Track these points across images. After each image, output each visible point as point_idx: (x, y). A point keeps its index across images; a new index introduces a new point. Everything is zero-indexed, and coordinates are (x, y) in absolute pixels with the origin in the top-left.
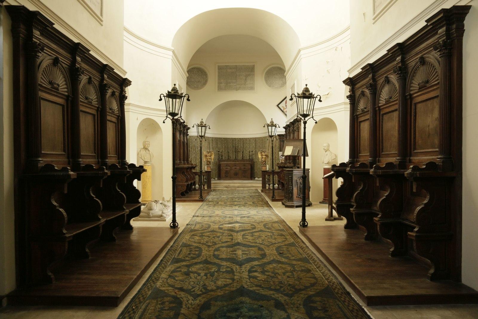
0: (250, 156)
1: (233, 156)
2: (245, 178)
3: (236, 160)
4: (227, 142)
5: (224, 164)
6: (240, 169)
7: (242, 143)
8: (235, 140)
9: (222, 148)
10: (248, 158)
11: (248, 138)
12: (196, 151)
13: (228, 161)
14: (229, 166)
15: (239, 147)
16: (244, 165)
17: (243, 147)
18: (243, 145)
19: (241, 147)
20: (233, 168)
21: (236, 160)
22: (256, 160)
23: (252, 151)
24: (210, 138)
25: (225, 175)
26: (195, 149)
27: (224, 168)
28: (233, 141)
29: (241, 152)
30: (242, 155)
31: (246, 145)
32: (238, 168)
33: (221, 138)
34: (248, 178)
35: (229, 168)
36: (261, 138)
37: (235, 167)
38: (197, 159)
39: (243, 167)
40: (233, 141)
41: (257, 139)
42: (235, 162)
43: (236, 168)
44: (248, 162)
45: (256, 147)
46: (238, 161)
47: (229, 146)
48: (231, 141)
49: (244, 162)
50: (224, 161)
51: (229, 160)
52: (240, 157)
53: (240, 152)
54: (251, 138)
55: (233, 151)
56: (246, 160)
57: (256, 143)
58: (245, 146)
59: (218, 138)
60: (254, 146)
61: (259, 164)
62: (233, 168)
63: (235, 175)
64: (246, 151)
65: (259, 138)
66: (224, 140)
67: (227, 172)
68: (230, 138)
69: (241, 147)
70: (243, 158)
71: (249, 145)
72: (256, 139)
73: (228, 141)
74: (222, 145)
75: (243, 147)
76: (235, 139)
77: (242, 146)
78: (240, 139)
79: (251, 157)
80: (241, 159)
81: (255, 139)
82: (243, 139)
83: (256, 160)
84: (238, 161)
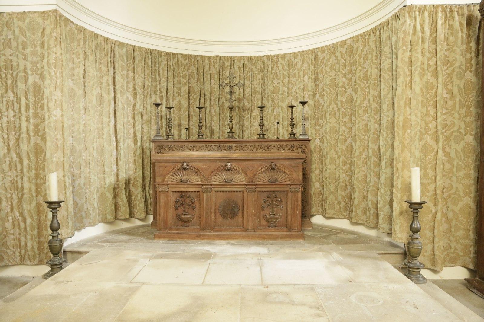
0: (293, 125)
1: (219, 127)
2: (273, 232)
3: (232, 140)
4: (198, 74)
5: (173, 160)
6: (251, 185)
7: (259, 77)
8: (232, 66)
9: (179, 94)
10: (284, 134)
11: (284, 56)
12: (16, 95)
13: (197, 145)
14: (197, 172)
15: (248, 91)
16: (272, 165)
17: (264, 91)
18: (263, 84)
19: (254, 92)
20: (217, 180)
21: (232, 140)
22: (317, 141)
23: (303, 103)
24: (121, 45)
25: (178, 215)
26: (15, 81)
27: (170, 179)
28: (222, 67)
29: (257, 112)
30: (257, 124)
31: (276, 81)
32: (240, 179)
33: (174, 55)
34: (290, 229)
35: (195, 179)
36: (343, 43)
37: (225, 176)
38: (24, 136)
39: (263, 178)
40: (222, 67)
41: (321, 56)
42: (230, 148)
43: (227, 183)
44: (285, 153)
45: (317, 86)
46: (242, 149)
47: (207, 88)
48: (217, 66)
49: (269, 148)
50: (180, 144)
51: (202, 140)
52: (251, 130)
53: (250, 110)
54: (295, 55)
55: (221, 108)
56: (278, 140)
57: (315, 73)
58: (271, 87)
59: (159, 53)
60: (311, 85)
61: (332, 161)
62: (217, 180)
63: (224, 217)
64: (275, 106)
65: (332, 49)
66: (185, 63)
67: (184, 201)
68: (209, 57)
69: (254, 92)
70: (262, 135)
71: (286, 80)
72: (317, 57)
73: (204, 67)
74: (179, 82)
75: (264, 91)
76: (232, 59)
77: (259, 89)
78: (251, 59)
79: (298, 130)
80: (256, 137)
81: (314, 56)
82: (261, 59)
83: (317, 141)
84: (242, 144)
